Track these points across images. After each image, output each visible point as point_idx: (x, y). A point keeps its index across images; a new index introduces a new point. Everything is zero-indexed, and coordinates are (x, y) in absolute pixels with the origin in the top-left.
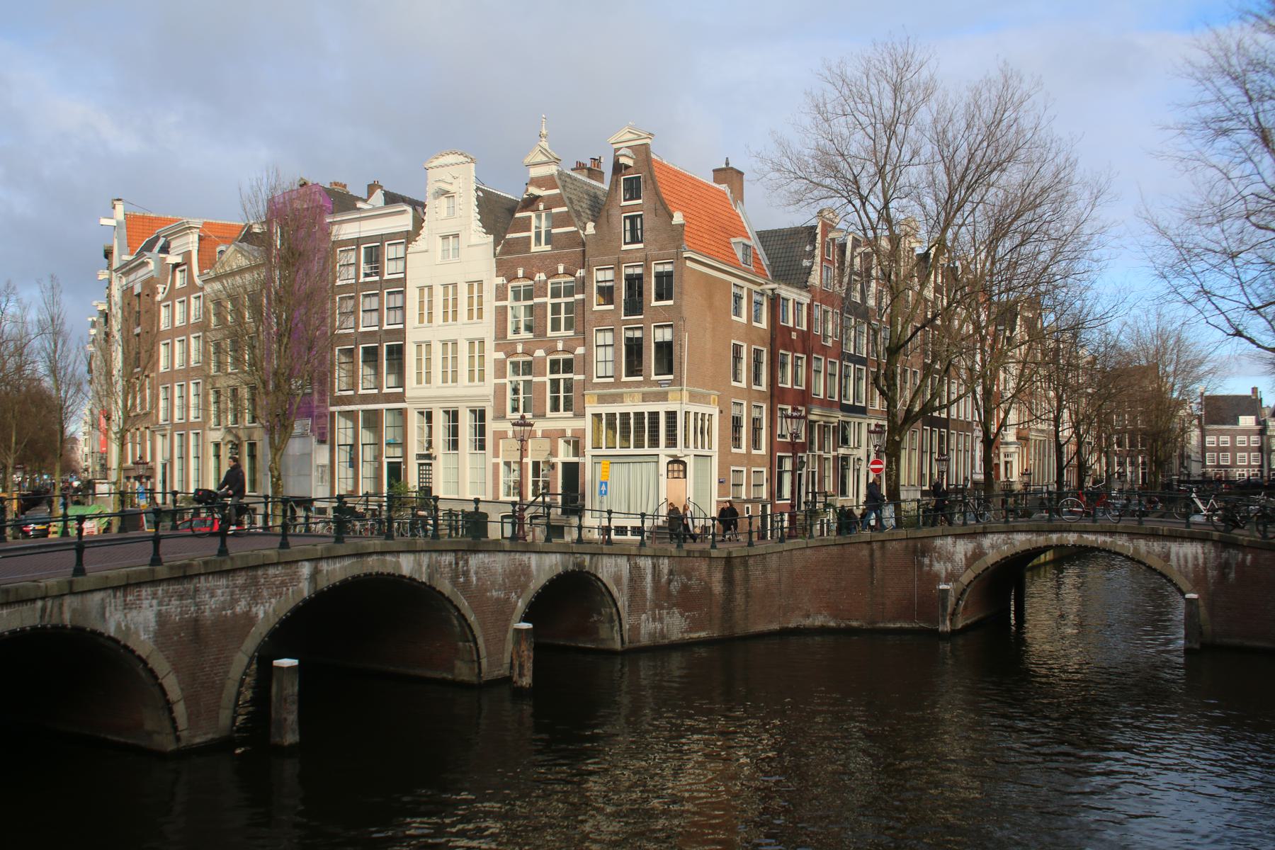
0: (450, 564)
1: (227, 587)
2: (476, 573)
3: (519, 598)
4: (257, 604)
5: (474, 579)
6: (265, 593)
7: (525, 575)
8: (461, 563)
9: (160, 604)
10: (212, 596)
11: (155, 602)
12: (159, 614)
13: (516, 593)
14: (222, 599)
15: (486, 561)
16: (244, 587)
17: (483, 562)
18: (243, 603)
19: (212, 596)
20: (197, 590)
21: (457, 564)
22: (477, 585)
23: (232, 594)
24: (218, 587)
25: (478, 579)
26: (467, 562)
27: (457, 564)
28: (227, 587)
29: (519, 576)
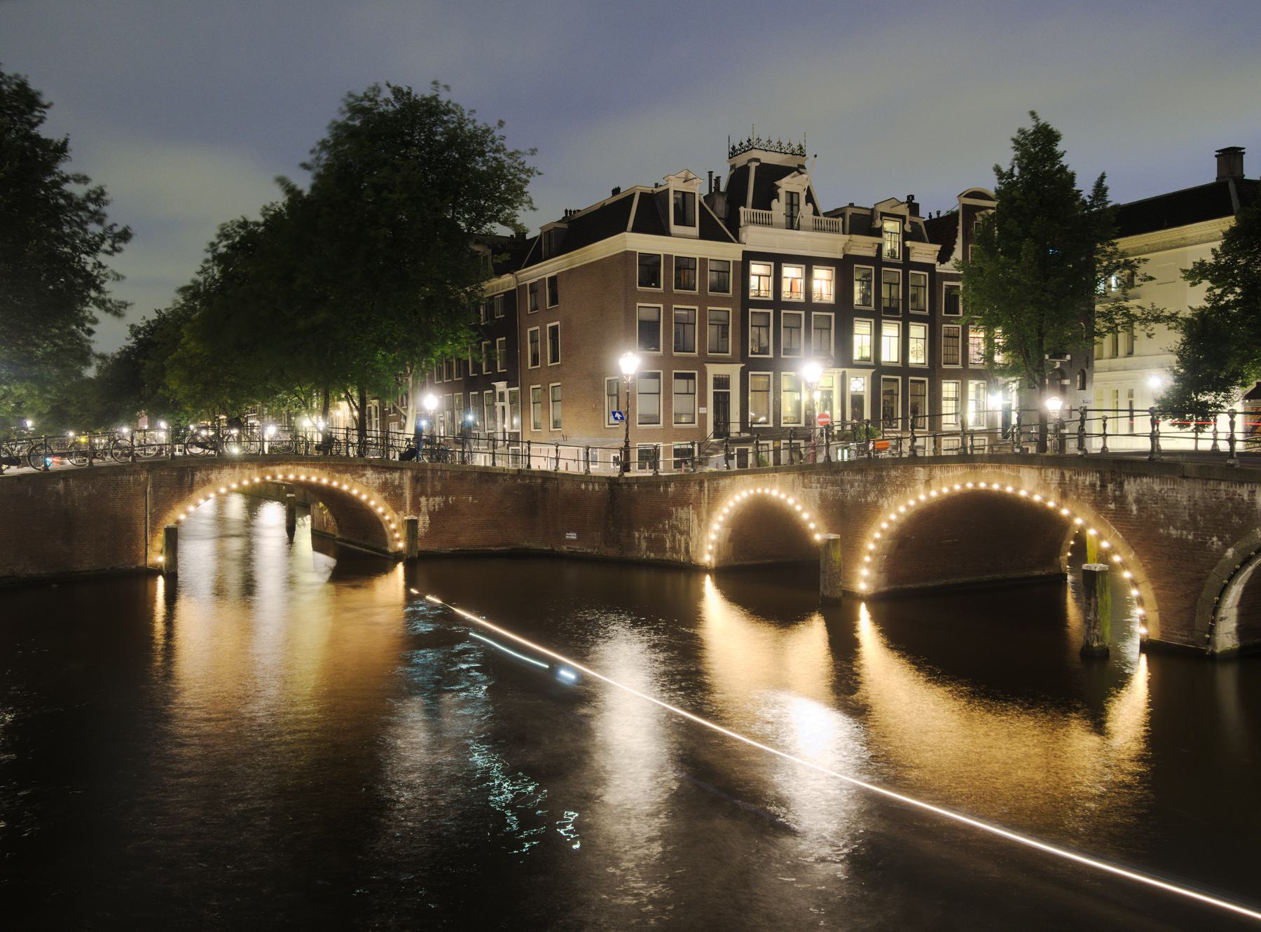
0: (1093, 485)
1: (862, 481)
2: (1138, 501)
3: (1226, 546)
4: (883, 497)
5: (1134, 508)
6: (889, 490)
7: (1241, 516)
8: (1110, 487)
9: (821, 487)
10: (852, 487)
11: (818, 485)
12: (821, 494)
13: (1220, 539)
14: (858, 489)
15: (1157, 488)
16: (873, 483)
17: (1152, 490)
18: (872, 495)
19: (852, 487)
20: (842, 481)
21: (1103, 486)
22: (1139, 517)
23: (865, 487)
24: (856, 481)
25: (1140, 509)
26: (1121, 485)
27: (1103, 486)
28: (862, 481)
29: (1229, 516)
